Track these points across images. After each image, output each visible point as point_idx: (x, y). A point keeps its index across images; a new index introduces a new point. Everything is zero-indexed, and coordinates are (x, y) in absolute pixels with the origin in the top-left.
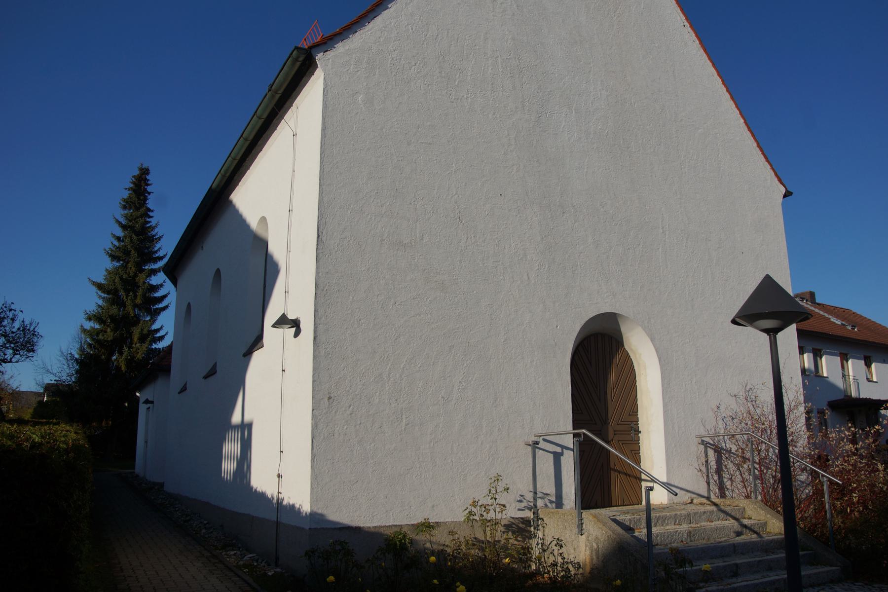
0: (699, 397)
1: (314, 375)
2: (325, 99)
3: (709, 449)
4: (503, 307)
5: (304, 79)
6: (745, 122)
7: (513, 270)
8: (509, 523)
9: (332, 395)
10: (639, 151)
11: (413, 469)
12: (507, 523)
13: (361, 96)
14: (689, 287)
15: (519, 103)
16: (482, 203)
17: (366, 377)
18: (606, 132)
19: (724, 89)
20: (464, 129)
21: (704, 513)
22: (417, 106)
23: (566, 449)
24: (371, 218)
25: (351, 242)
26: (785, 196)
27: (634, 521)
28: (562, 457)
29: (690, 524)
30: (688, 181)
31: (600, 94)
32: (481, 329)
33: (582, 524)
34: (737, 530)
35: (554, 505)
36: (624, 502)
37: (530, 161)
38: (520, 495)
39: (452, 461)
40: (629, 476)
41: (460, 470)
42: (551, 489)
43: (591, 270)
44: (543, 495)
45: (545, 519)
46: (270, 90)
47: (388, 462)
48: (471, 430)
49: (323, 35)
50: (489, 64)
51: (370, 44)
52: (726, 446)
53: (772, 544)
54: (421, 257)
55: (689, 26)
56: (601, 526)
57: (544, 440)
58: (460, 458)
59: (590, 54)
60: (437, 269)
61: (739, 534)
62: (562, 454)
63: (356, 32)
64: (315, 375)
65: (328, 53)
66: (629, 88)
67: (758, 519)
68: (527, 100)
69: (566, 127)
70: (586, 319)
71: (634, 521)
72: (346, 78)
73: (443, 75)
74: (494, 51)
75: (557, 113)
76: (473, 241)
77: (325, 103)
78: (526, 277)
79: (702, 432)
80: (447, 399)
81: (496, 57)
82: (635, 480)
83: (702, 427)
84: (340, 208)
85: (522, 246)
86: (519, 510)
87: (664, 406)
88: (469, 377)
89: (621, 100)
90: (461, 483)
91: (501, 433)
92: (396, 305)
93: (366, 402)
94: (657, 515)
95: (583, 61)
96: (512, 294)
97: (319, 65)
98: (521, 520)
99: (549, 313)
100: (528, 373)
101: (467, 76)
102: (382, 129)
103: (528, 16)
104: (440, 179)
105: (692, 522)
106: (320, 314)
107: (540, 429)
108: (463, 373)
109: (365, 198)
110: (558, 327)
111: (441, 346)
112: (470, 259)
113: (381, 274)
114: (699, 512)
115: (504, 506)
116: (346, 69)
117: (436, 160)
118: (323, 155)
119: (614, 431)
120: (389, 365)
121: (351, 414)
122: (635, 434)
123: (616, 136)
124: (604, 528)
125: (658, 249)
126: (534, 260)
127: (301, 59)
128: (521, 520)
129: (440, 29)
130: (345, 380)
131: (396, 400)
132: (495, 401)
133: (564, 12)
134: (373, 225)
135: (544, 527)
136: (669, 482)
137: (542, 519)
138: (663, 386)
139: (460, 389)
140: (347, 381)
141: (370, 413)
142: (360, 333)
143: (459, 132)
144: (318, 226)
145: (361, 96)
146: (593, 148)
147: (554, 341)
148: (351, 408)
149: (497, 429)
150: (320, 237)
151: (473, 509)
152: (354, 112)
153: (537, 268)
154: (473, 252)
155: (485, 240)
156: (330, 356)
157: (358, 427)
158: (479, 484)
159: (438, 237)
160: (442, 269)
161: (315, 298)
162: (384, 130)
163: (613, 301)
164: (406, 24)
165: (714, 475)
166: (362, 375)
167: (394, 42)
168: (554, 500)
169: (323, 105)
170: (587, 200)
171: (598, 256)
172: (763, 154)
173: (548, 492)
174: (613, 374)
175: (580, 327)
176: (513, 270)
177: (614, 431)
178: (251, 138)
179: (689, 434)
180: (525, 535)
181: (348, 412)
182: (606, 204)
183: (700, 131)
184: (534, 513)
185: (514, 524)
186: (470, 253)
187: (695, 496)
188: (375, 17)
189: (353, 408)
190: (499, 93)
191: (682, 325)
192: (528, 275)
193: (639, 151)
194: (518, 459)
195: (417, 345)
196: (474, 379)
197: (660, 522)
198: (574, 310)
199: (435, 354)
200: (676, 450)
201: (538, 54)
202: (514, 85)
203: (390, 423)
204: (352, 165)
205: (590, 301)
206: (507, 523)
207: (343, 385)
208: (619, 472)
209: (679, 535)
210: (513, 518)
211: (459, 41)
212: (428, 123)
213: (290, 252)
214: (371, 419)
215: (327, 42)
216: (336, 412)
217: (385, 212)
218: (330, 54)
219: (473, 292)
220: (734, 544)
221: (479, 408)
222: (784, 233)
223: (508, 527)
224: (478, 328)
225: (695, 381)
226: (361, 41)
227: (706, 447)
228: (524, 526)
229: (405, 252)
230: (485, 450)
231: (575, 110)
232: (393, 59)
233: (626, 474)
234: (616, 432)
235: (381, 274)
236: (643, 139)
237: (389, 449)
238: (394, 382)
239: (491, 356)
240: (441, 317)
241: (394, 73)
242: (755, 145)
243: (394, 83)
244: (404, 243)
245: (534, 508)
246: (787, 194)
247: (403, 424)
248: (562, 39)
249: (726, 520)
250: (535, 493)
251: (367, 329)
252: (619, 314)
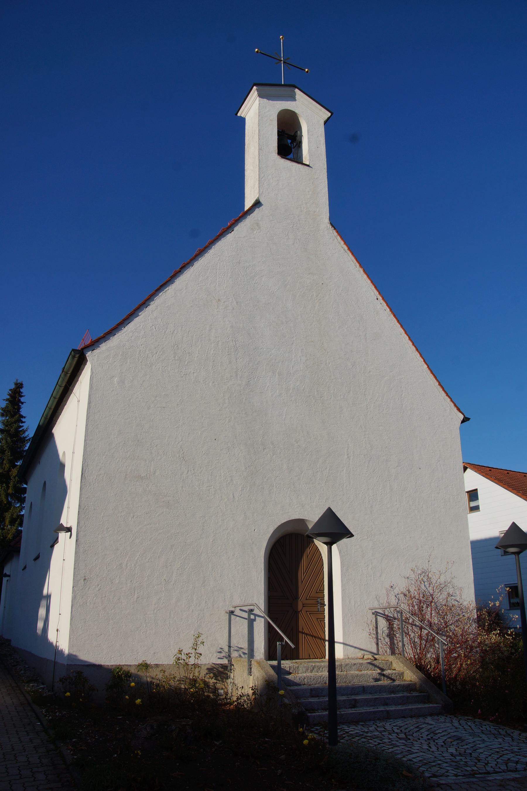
0: (374, 579)
1: (75, 564)
2: (91, 383)
3: (378, 617)
4: (213, 517)
5: (82, 366)
6: (428, 367)
7: (222, 491)
8: (211, 667)
9: (87, 578)
10: (331, 399)
11: (140, 628)
12: (209, 667)
13: (116, 379)
14: (369, 497)
15: (234, 373)
16: (200, 446)
17: (111, 566)
18: (303, 387)
19: (411, 343)
20: (190, 395)
21: (355, 664)
22: (156, 382)
23: (258, 617)
24: (119, 461)
25: (104, 477)
26: (463, 421)
27: (293, 668)
28: (254, 622)
29: (342, 671)
30: (372, 418)
31: (300, 360)
32: (195, 533)
33: (251, 668)
34: (376, 677)
35: (246, 656)
36: (310, 656)
37: (240, 414)
38: (220, 648)
39: (170, 623)
40: (315, 637)
41: (175, 630)
42: (245, 645)
43: (285, 489)
44: (238, 649)
45: (235, 665)
46: (62, 372)
47: (123, 622)
48: (185, 602)
49: (92, 340)
50: (212, 347)
51: (124, 342)
52: (398, 616)
53: (399, 688)
54: (154, 485)
55: (381, 298)
56: (260, 670)
57: (241, 610)
58: (175, 621)
59: (293, 330)
60: (165, 493)
61: (376, 680)
62: (255, 620)
63: (115, 335)
64: (76, 564)
65: (95, 351)
66: (325, 352)
67: (399, 670)
68: (240, 370)
69: (270, 387)
70: (279, 524)
71: (293, 668)
72: (106, 367)
73: (176, 358)
74: (216, 337)
75: (263, 377)
76: (192, 473)
77: (91, 385)
78: (231, 496)
79: (376, 605)
80: (168, 581)
81: (218, 342)
82: (319, 640)
83: (376, 602)
84: (98, 455)
85: (230, 474)
86: (219, 658)
87: (342, 587)
88: (185, 566)
89: (318, 362)
90: (176, 638)
91: (207, 605)
92: (134, 518)
93: (110, 582)
94: (313, 665)
95: (287, 336)
96: (220, 508)
97: (88, 360)
98: (220, 666)
99: (248, 521)
100: (230, 563)
101: (195, 357)
102: (130, 400)
103: (245, 308)
104: (170, 431)
105: (343, 670)
106: (81, 525)
107: (237, 601)
108: (180, 563)
109: (116, 448)
110: (256, 530)
111: (165, 545)
112: (190, 485)
113: (124, 498)
114: (350, 663)
115: (201, 654)
116: (106, 361)
117: (168, 418)
118: (88, 421)
119: (303, 604)
120: (127, 558)
121: (99, 590)
122: (321, 607)
123: (311, 389)
124: (261, 671)
125: (343, 470)
126: (238, 484)
127: (77, 356)
128: (220, 666)
129: (176, 326)
130: (96, 568)
131: (131, 581)
132: (204, 582)
133: (274, 302)
134: (120, 465)
135: (234, 671)
136: (345, 642)
137: (233, 665)
138: (342, 571)
139: (177, 574)
140: (97, 568)
141: (112, 590)
142: (108, 537)
143: (186, 397)
144: (82, 467)
145: (116, 379)
146: (291, 400)
147: (252, 540)
148: (99, 586)
149: (204, 601)
150: (83, 475)
151: (180, 656)
152: (111, 389)
153: (241, 489)
154: (192, 481)
155: (201, 472)
156: (87, 552)
157: (103, 598)
158: (189, 639)
159: (167, 471)
160: (168, 493)
161: (78, 514)
162: (131, 401)
164: (152, 325)
165: (386, 638)
166: (108, 565)
167: (142, 339)
168: (247, 652)
169: (90, 386)
170: (284, 438)
171: (291, 479)
172: (444, 390)
173: (242, 647)
174: (304, 562)
175: (273, 530)
176: (222, 491)
178: (58, 396)
179: (364, 607)
180: (223, 676)
181: (97, 589)
182: (300, 440)
183: (386, 378)
184: (228, 661)
185: (215, 668)
186: (190, 481)
187: (366, 653)
188: (129, 323)
189: (101, 586)
190: (218, 367)
191: (362, 526)
192: (233, 494)
193: (331, 399)
194: (220, 623)
195: (147, 545)
196: (188, 567)
197: (315, 669)
198: (269, 518)
199: (160, 550)
200: (351, 619)
201: (251, 335)
202: (230, 360)
203: (126, 596)
204: (108, 425)
205: (282, 511)
206: (209, 667)
207: (94, 571)
208: (307, 634)
209: (323, 678)
210: (214, 664)
211: (190, 333)
212: (164, 393)
213: (72, 480)
214: (113, 594)
215: (94, 344)
216: (89, 589)
217: (129, 456)
218: (97, 351)
219: (191, 507)
220: (363, 687)
221: (191, 587)
222: (461, 451)
223: (210, 670)
224: (193, 533)
225: (371, 568)
226: (118, 340)
227: (376, 615)
228: (223, 670)
229: (142, 482)
230: (194, 616)
231: (278, 373)
232: (140, 351)
233: (312, 636)
234: (304, 605)
235: (124, 498)
236: (334, 389)
237: (125, 613)
238: (130, 569)
239: (202, 552)
240: (166, 526)
241: (140, 361)
242: (437, 383)
243: (140, 368)
244: (142, 476)
245: (229, 657)
246: (465, 419)
247: (136, 597)
248: (272, 322)
249: (374, 670)
250: (230, 647)
251: (113, 534)
252: (307, 520)
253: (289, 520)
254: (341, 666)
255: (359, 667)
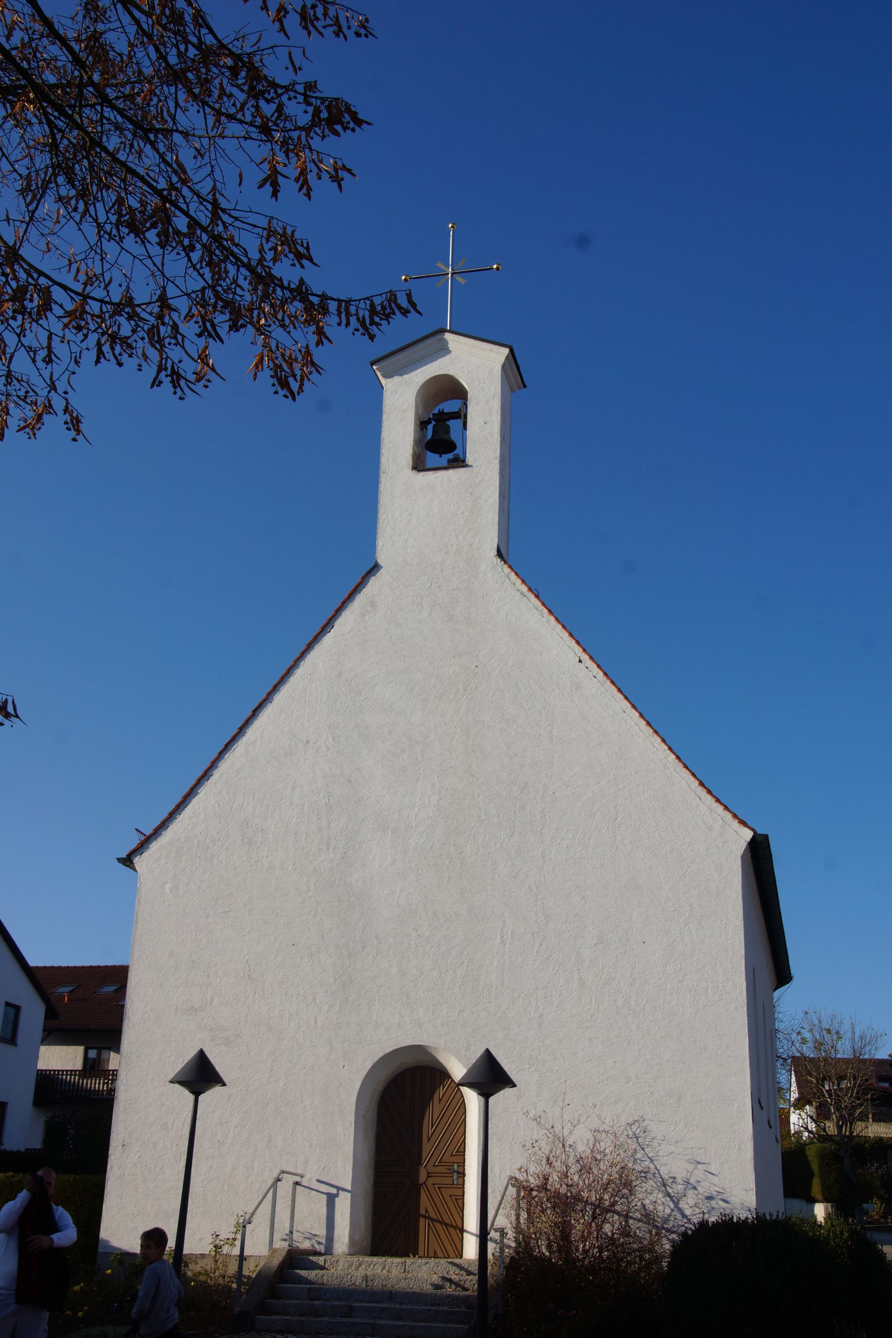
9: (126, 1143)
10: (477, 852)
18: (431, 843)
30: (553, 870)
31: (429, 801)
34: (436, 1282)
39: (222, 1199)
43: (393, 1003)
53: (450, 1300)
62: (337, 1195)
66: (473, 780)
78: (313, 1022)
96: (296, 1040)
105: (407, 1271)
119: (428, 1173)
121: (139, 1158)
125: (491, 964)
149: (268, 1169)
157: (144, 1168)
163: (419, 1031)
173: (317, 1233)
177: (428, 1173)
181: (137, 1157)
182: (420, 926)
192: (315, 1019)
193: (477, 852)
196: (249, 1124)
209: (351, 1277)
212: (227, 893)
216: (127, 1157)
218: (145, 855)
234: (430, 1175)
236: (485, 836)
253: (397, 1048)
254: (404, 1264)
255: (434, 1267)
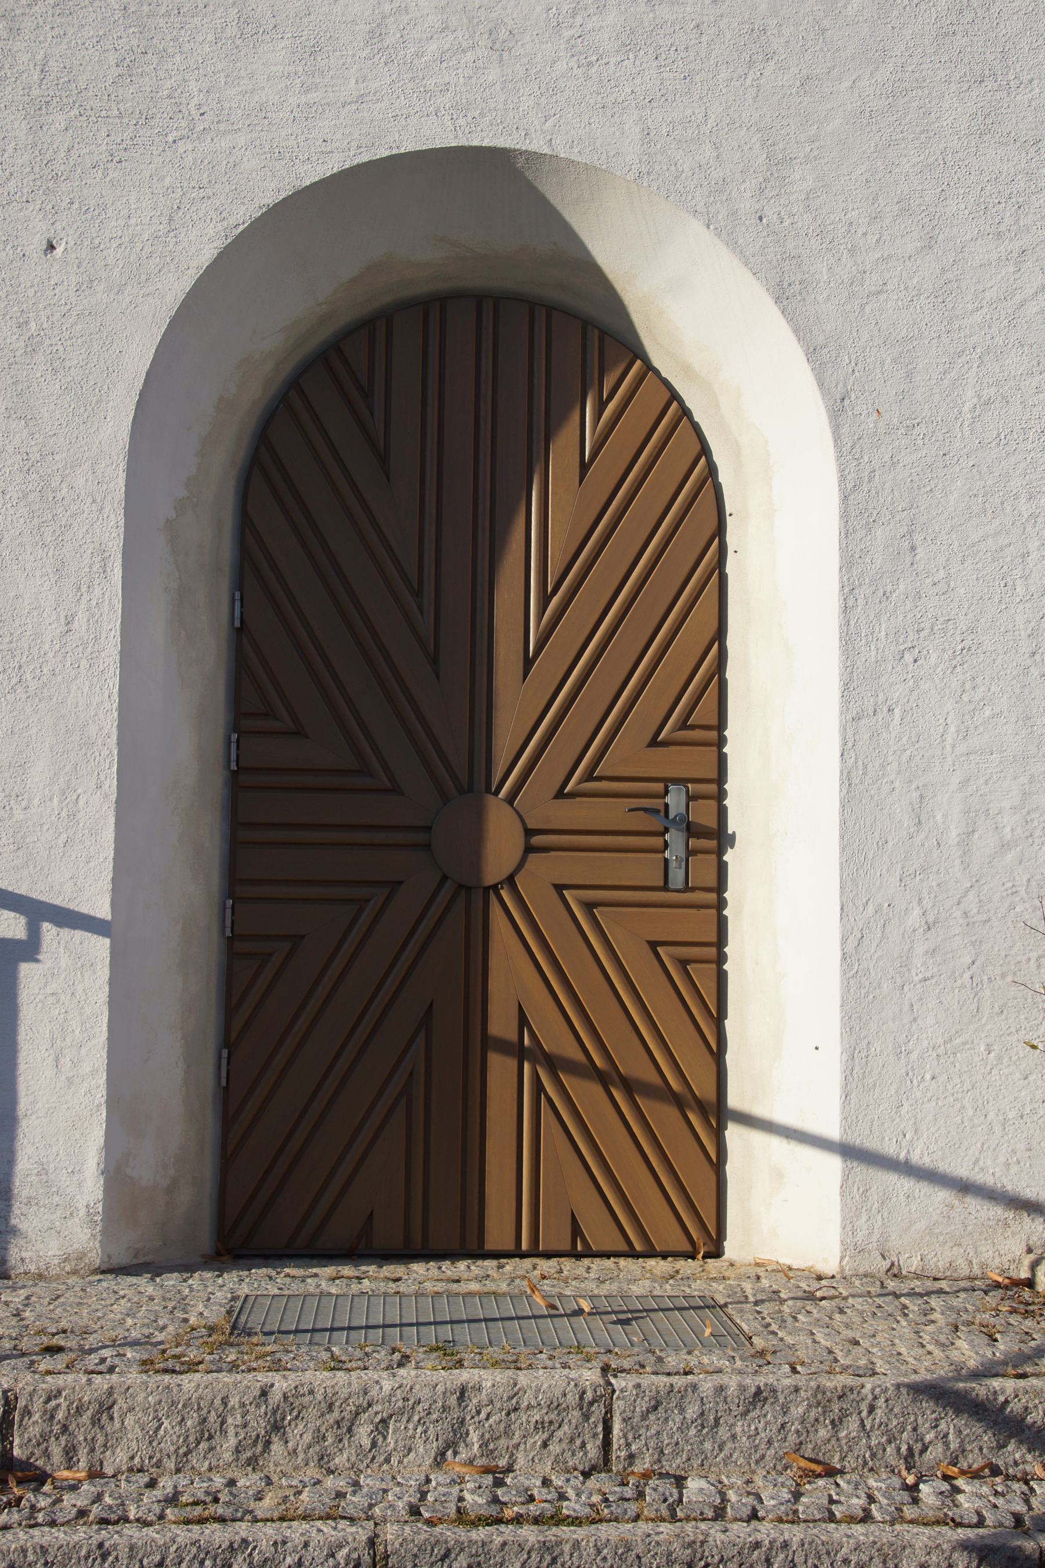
28: (25, 969)
82: (671, 1112)
87: (846, 687)
94: (281, 1384)
105: (618, 1452)
119: (529, 833)
136: (861, 1139)
138: (848, 562)
163: (493, 75)
175: (220, 244)
177: (529, 833)
253: (365, 158)
254: (598, 1411)
255: (808, 1426)
